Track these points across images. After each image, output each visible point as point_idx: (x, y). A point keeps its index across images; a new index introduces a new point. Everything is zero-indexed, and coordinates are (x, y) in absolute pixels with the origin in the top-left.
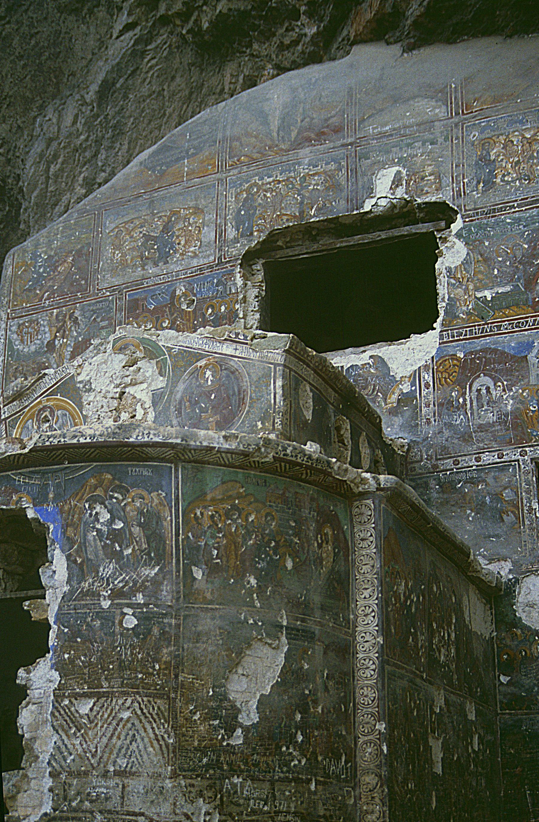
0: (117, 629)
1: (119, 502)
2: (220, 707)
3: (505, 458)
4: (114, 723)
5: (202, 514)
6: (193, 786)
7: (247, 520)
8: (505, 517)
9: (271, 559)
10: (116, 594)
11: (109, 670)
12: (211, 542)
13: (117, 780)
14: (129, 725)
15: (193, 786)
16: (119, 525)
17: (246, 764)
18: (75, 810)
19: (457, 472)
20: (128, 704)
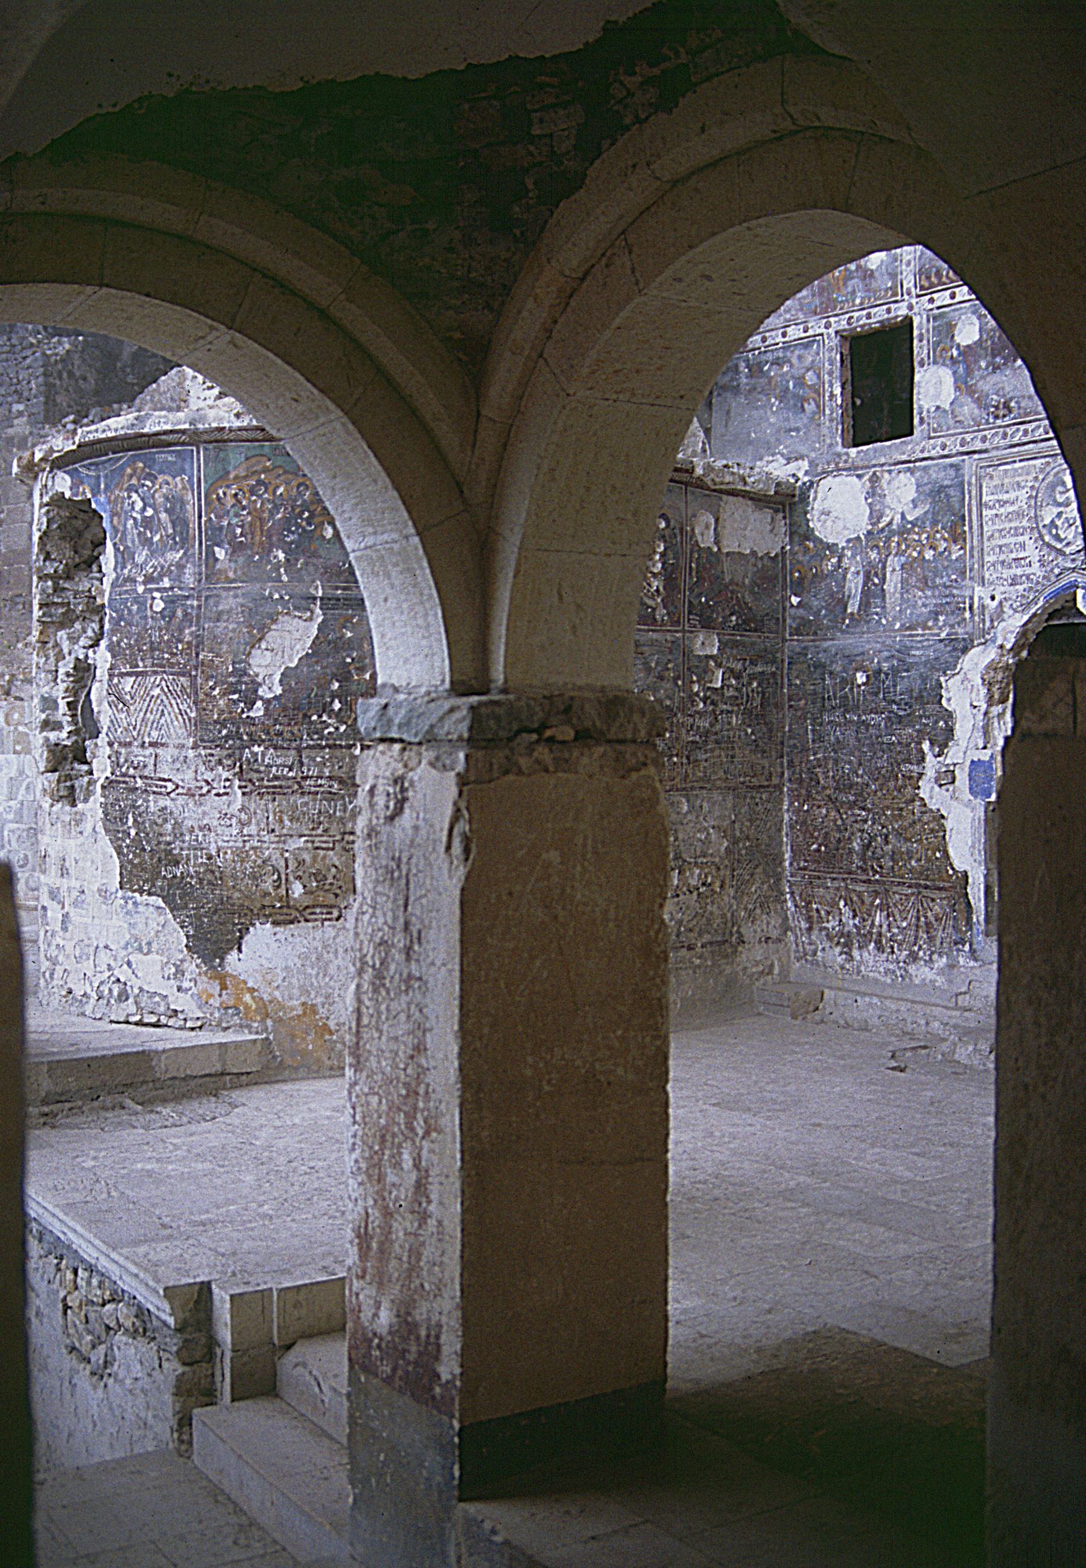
0: (149, 613)
1: (149, 489)
2: (239, 682)
3: (810, 332)
4: (148, 699)
5: (225, 494)
6: (212, 755)
7: (274, 493)
8: (806, 405)
9: (304, 529)
10: (149, 579)
11: (143, 651)
12: (234, 521)
13: (151, 750)
14: (159, 701)
15: (212, 755)
16: (149, 512)
17: (268, 733)
18: (124, 775)
19: (765, 352)
20: (157, 683)
